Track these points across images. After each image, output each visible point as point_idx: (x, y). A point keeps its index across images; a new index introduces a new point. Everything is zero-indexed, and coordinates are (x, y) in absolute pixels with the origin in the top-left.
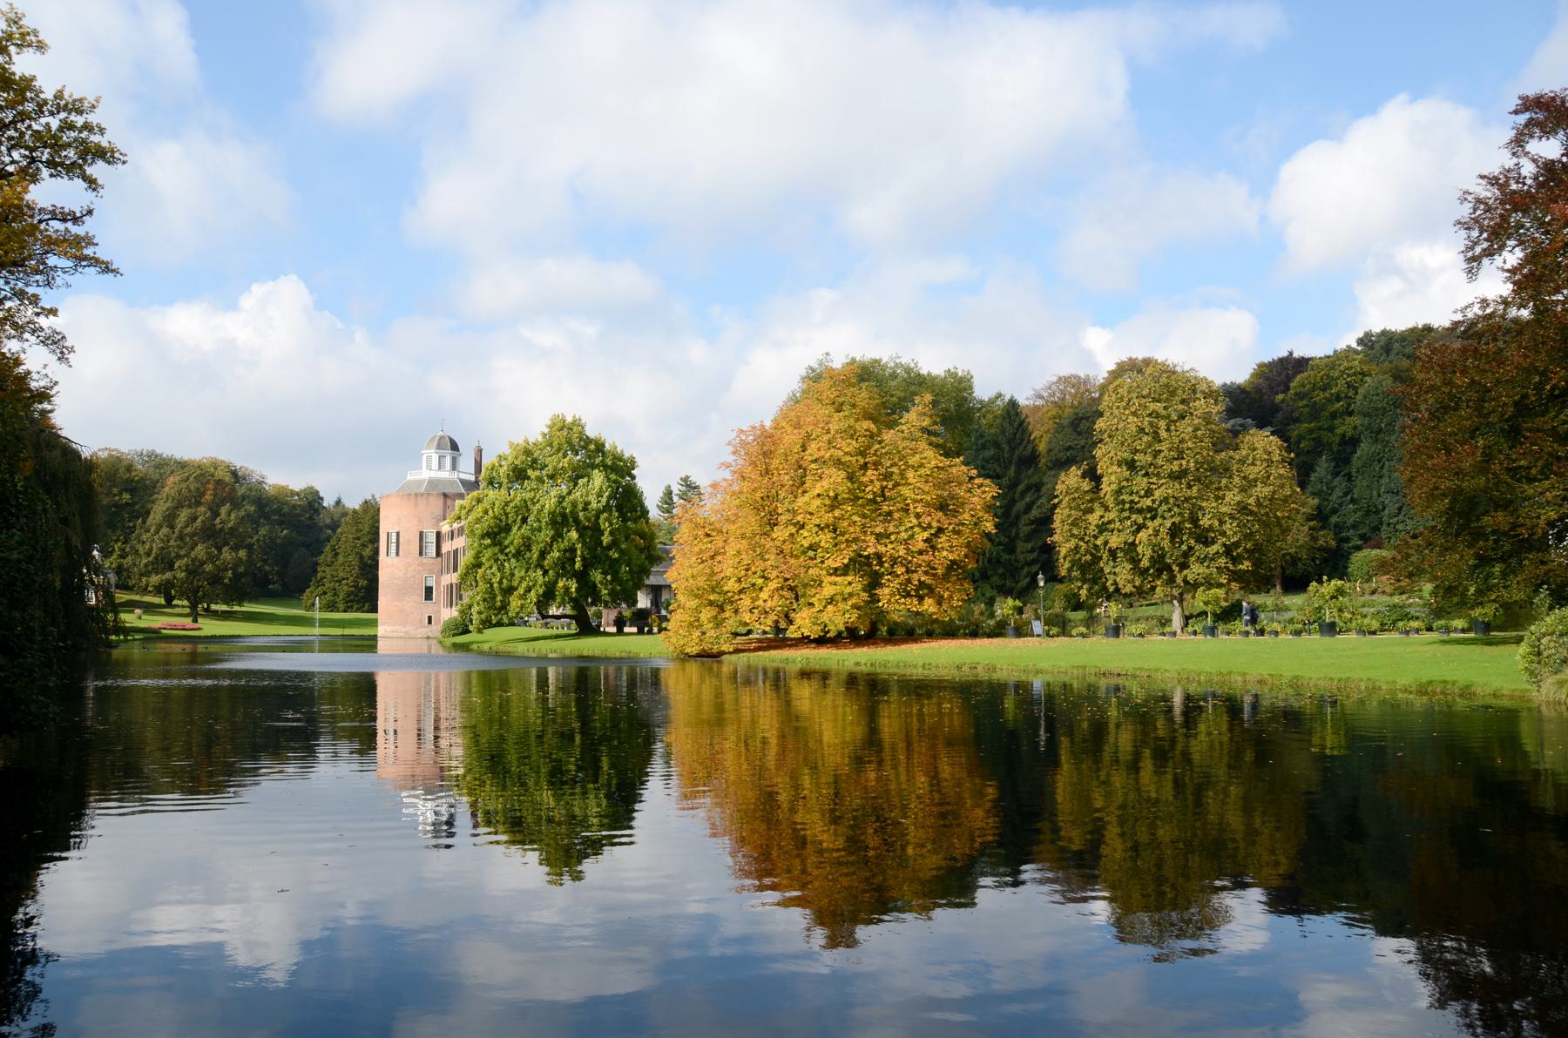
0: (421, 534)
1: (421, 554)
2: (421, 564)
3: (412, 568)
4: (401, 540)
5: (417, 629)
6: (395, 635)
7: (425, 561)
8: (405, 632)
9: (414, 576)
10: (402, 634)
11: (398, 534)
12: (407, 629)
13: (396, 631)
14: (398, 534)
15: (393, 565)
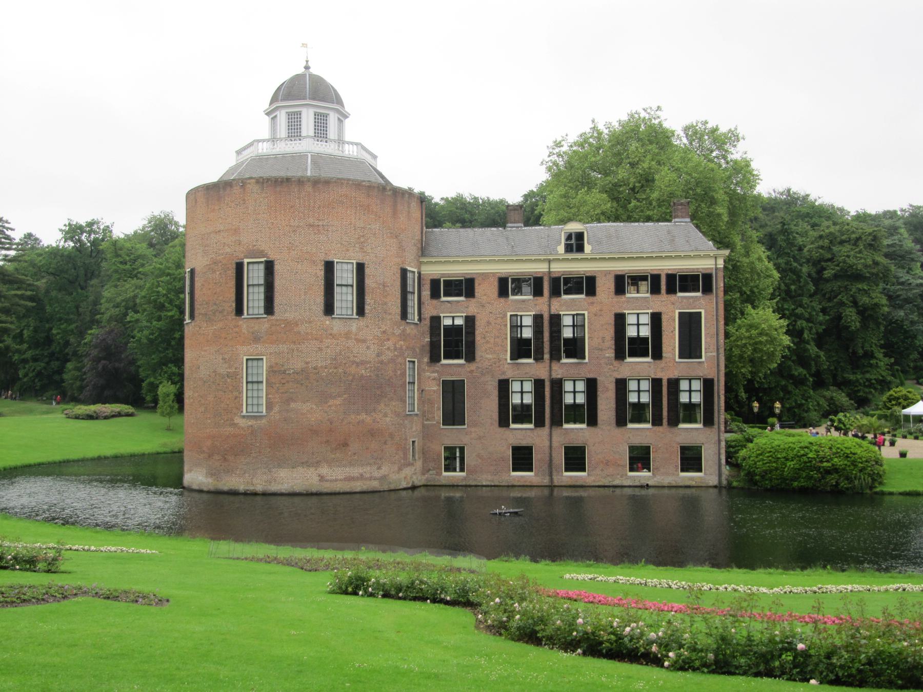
0: (404, 272)
1: (404, 315)
2: (404, 336)
3: (390, 344)
4: (369, 282)
5: (400, 469)
6: (358, 486)
7: (409, 330)
8: (383, 478)
9: (392, 360)
10: (375, 485)
11: (361, 268)
12: (385, 470)
13: (361, 477)
14: (361, 268)
15: (347, 335)
